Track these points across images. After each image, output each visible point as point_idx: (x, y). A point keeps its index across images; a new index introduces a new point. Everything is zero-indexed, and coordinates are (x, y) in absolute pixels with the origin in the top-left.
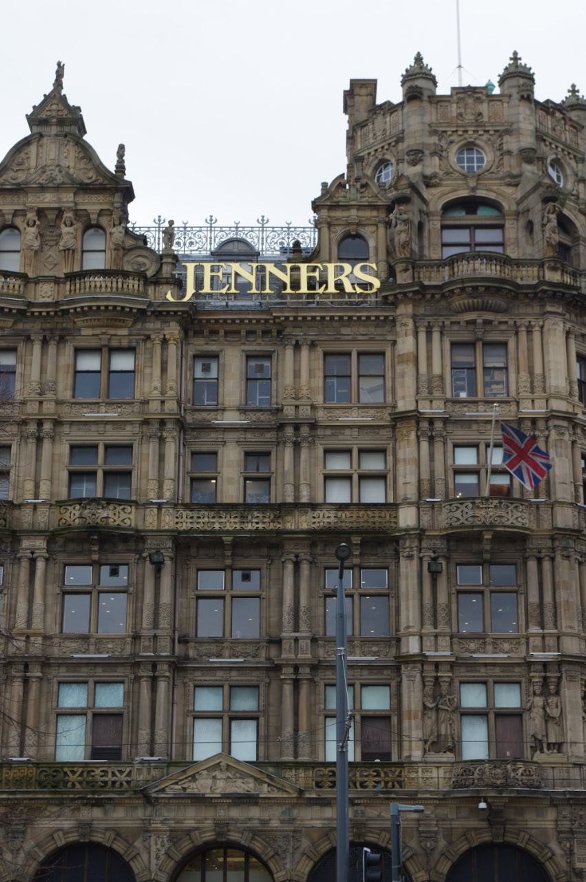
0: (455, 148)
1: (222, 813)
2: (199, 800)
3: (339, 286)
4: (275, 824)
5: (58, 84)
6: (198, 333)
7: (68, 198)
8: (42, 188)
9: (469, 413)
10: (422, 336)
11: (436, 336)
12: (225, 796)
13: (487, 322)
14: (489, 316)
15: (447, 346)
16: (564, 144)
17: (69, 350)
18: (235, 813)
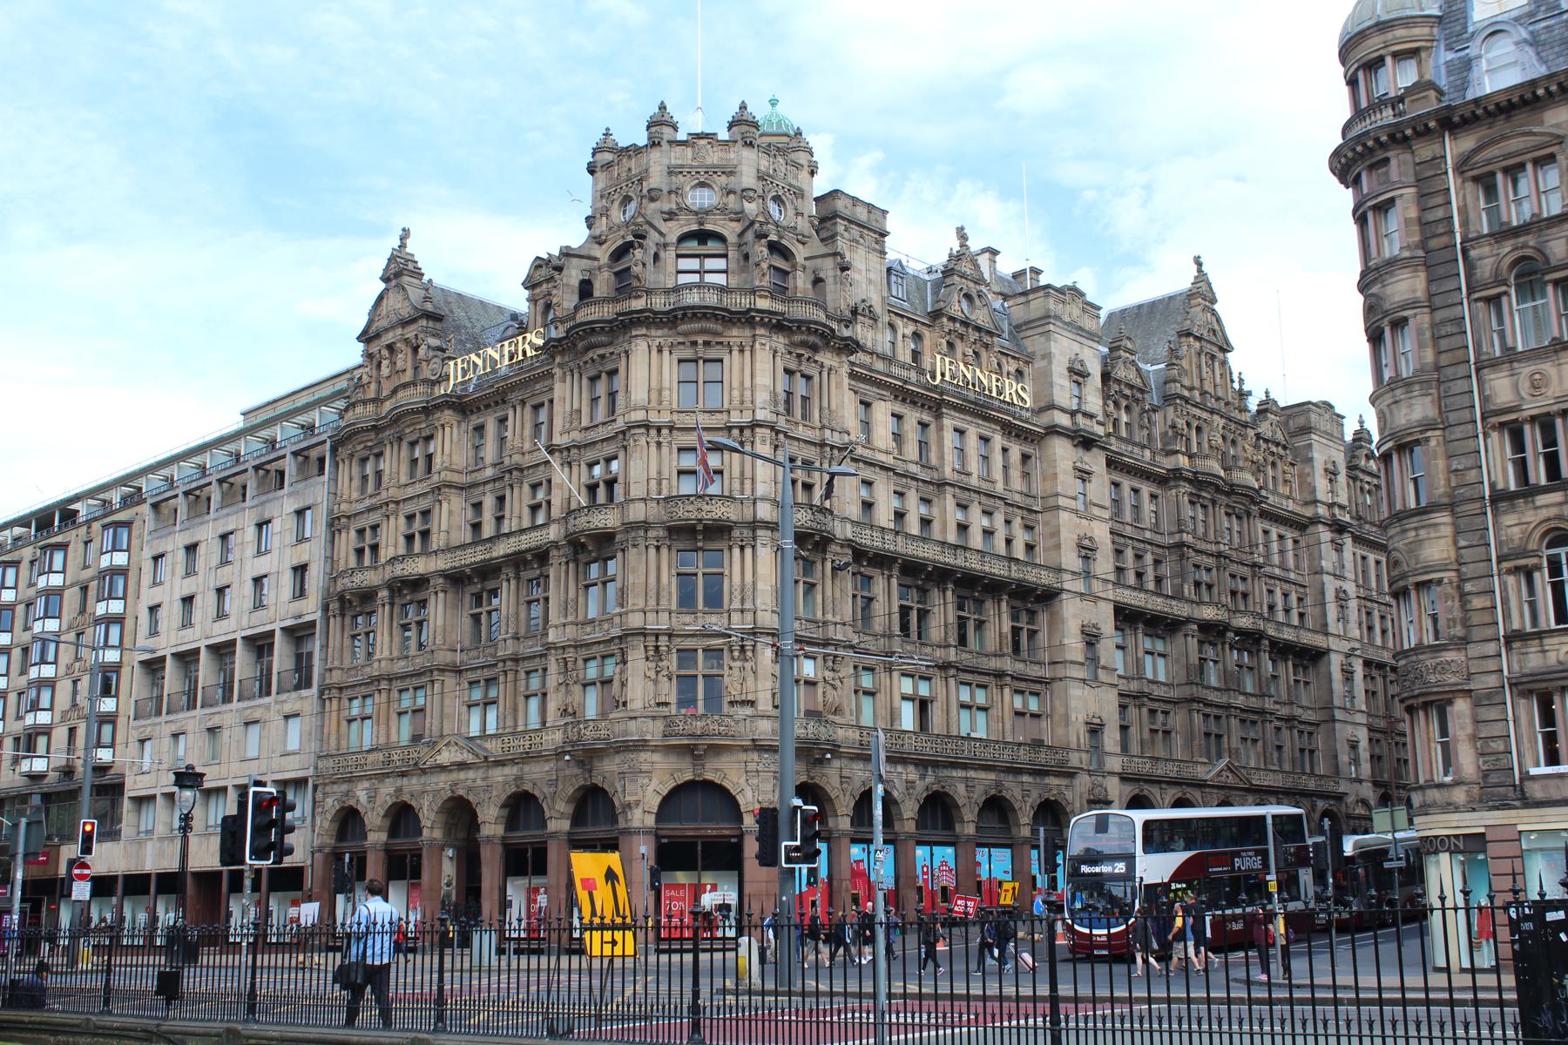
0: (617, 204)
1: (454, 776)
2: (442, 768)
3: (524, 353)
4: (479, 782)
5: (403, 246)
6: (472, 412)
7: (399, 331)
8: (387, 330)
9: (593, 435)
10: (568, 378)
11: (576, 376)
12: (453, 764)
13: (602, 357)
14: (601, 351)
15: (585, 381)
16: (714, 166)
17: (405, 445)
18: (462, 775)
